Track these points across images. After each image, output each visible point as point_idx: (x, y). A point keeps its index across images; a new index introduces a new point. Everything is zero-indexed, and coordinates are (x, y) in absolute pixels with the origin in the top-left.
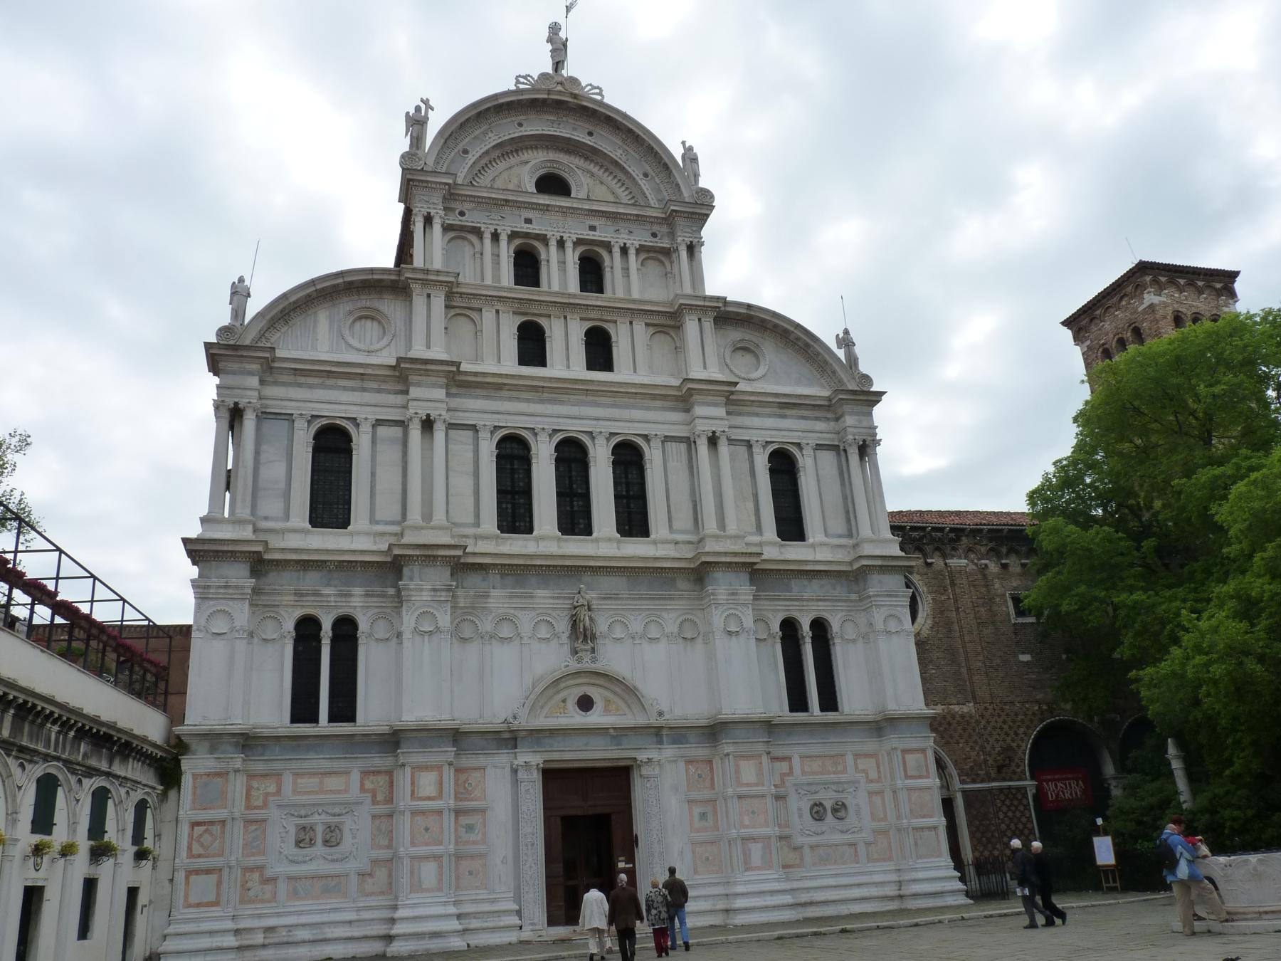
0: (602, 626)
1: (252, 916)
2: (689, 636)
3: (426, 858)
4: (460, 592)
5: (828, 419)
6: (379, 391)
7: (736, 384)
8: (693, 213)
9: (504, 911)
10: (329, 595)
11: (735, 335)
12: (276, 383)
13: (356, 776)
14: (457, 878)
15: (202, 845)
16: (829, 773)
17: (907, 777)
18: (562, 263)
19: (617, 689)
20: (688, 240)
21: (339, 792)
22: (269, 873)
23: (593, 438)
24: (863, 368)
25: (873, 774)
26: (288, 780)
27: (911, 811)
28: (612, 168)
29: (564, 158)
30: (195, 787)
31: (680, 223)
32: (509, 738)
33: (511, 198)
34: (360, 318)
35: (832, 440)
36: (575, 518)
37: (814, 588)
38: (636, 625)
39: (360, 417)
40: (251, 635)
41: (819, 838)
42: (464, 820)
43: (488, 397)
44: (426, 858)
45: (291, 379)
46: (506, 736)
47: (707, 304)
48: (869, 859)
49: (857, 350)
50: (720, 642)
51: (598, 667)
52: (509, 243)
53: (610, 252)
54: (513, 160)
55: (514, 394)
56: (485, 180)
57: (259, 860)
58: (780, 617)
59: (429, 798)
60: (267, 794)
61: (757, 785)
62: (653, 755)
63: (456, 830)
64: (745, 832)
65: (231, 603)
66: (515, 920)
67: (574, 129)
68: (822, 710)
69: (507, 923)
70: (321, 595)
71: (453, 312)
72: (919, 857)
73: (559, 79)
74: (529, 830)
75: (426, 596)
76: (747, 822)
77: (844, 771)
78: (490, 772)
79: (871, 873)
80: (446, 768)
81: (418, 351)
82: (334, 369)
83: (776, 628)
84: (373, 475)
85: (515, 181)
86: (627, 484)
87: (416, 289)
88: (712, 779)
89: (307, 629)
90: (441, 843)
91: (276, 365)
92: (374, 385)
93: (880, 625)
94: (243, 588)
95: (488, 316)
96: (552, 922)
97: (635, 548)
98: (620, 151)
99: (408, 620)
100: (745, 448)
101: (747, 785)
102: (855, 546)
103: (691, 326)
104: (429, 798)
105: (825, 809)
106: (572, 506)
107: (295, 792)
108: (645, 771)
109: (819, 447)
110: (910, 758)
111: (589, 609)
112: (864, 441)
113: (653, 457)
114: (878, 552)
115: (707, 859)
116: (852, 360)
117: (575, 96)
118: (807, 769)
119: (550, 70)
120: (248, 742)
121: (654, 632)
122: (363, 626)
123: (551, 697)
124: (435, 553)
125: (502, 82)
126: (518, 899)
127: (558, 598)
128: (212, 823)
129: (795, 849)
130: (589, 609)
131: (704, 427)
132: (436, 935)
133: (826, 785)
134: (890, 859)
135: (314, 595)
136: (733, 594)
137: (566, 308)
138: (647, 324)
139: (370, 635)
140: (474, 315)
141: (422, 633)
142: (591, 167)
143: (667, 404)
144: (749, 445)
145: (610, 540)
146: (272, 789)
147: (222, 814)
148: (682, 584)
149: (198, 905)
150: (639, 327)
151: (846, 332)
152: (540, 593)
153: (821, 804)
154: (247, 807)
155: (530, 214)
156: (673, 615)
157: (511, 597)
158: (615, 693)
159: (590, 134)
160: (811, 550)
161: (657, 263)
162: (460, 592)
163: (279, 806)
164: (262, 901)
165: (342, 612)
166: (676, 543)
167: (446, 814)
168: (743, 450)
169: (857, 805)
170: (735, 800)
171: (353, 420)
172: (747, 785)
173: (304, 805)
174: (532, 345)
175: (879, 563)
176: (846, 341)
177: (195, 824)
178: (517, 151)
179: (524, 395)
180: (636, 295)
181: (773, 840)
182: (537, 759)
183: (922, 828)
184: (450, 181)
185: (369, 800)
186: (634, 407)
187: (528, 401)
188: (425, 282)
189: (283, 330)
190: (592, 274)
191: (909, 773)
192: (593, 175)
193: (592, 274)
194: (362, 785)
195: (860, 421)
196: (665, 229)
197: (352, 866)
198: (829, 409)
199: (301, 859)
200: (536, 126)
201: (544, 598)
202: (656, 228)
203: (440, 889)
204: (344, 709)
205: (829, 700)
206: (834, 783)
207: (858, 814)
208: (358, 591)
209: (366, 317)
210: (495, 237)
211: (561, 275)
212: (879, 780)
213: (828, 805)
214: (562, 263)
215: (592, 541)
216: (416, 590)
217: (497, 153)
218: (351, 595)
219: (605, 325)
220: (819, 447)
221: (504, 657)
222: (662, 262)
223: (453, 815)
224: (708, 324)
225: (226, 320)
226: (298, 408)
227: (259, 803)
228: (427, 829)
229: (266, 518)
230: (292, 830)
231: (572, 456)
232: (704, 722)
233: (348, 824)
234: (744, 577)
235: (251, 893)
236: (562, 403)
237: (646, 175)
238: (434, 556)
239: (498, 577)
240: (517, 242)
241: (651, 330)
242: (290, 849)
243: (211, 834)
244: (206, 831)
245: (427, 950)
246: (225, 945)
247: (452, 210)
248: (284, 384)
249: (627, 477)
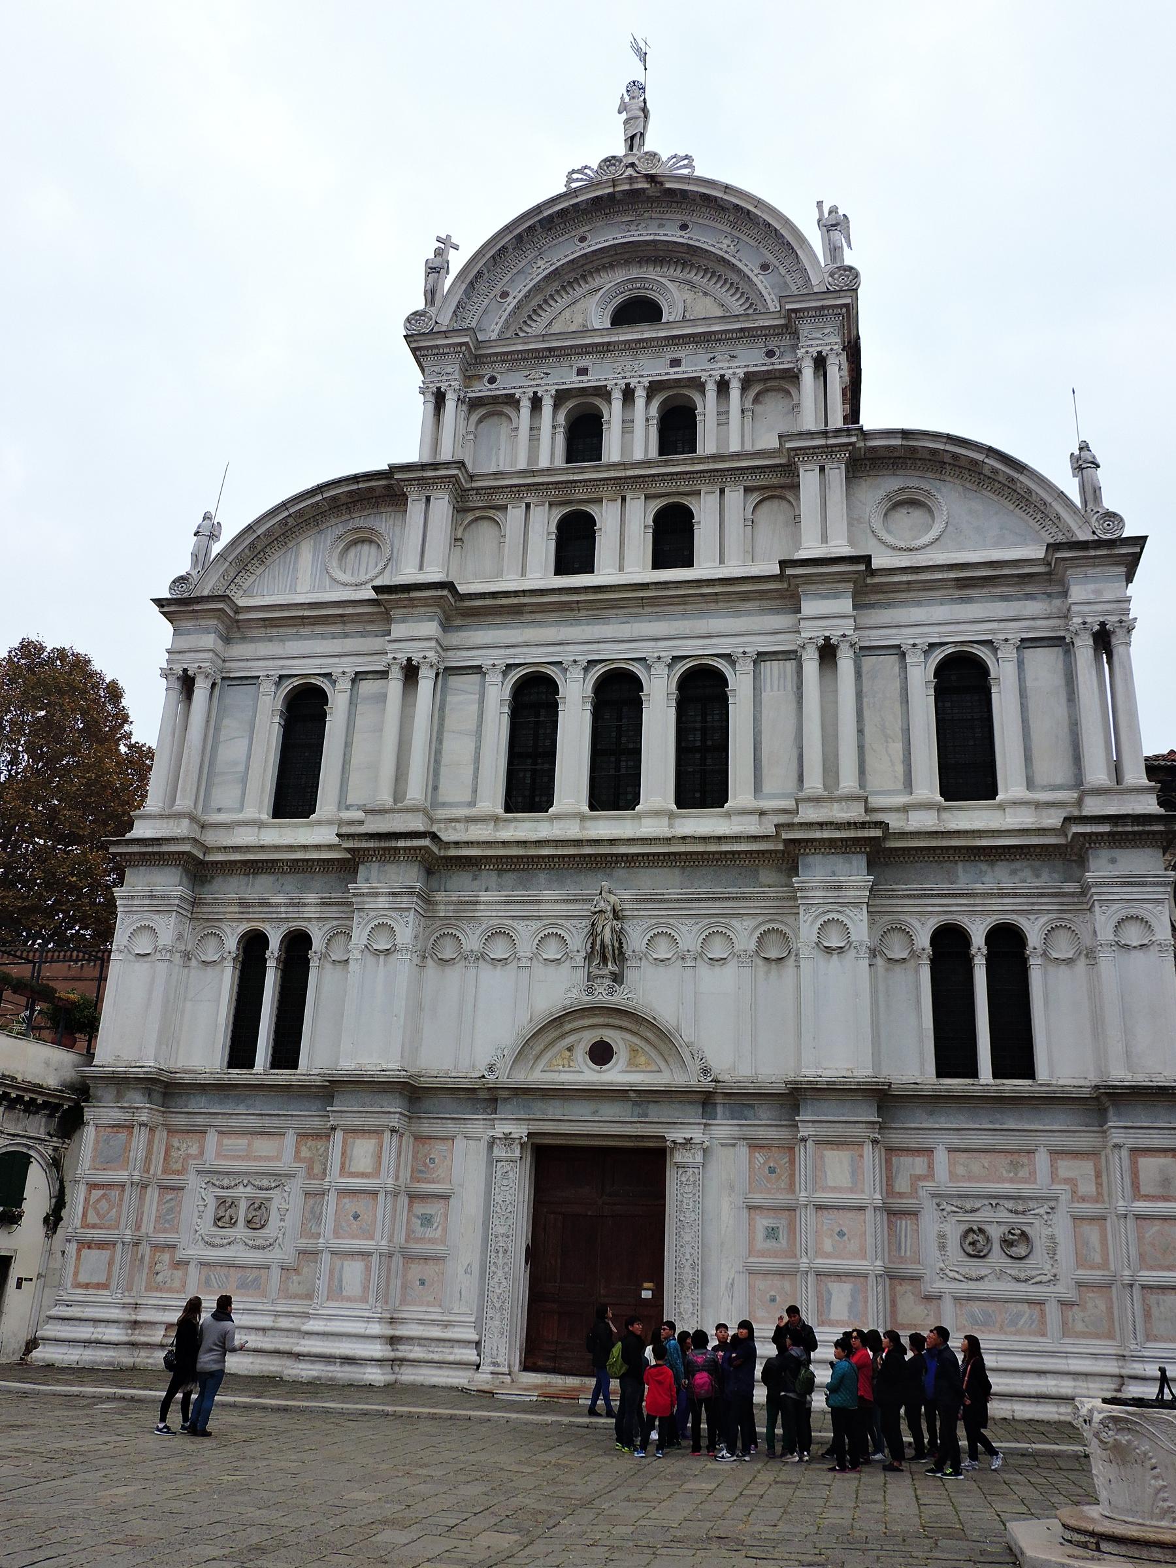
0: (636, 940)
1: (157, 1307)
2: (773, 954)
3: (351, 1254)
4: (439, 896)
5: (1049, 595)
6: (363, 635)
7: (867, 559)
8: (823, 308)
9: (458, 1341)
10: (279, 905)
11: (890, 483)
12: (244, 639)
13: (290, 1139)
14: (404, 1287)
15: (98, 1214)
16: (1001, 1180)
17: (1137, 1194)
18: (627, 423)
19: (649, 1035)
20: (814, 351)
21: (268, 1159)
22: (180, 1255)
23: (649, 667)
24: (1109, 502)
25: (1087, 1188)
26: (212, 1138)
27: (1141, 1256)
28: (720, 269)
29: (651, 273)
30: (97, 1142)
31: (804, 329)
32: (485, 1097)
34: (355, 543)
35: (1053, 629)
36: (614, 785)
37: (998, 877)
38: (689, 936)
39: (336, 672)
40: (187, 956)
41: (972, 1285)
42: (420, 1208)
43: (504, 625)
44: (351, 1254)
45: (261, 632)
46: (483, 1095)
47: (831, 441)
48: (1066, 1330)
49: (1103, 476)
50: (811, 964)
51: (618, 999)
52: (556, 407)
53: (703, 393)
54: (579, 291)
55: (538, 616)
56: (537, 328)
57: (171, 1237)
58: (933, 923)
59: (363, 1175)
60: (189, 1156)
61: (851, 1190)
62: (696, 1134)
63: (408, 1222)
64: (822, 1263)
65: (156, 917)
66: (470, 1355)
67: (661, 226)
68: (995, 1076)
69: (458, 1358)
70: (269, 905)
71: (470, 517)
72: (1149, 1337)
73: (631, 160)
74: (502, 1230)
75: (383, 902)
76: (828, 1245)
77: (1032, 1177)
78: (460, 1143)
79: (1066, 1355)
80: (387, 1134)
81: (408, 574)
82: (307, 613)
83: (923, 940)
84: (348, 745)
85: (579, 319)
86: (704, 731)
87: (412, 492)
88: (792, 1175)
89: (254, 944)
90: (373, 1239)
91: (241, 617)
92: (359, 628)
93: (1106, 933)
94: (169, 897)
95: (515, 513)
96: (527, 1367)
97: (702, 823)
98: (727, 241)
99: (360, 935)
100: (894, 659)
101: (834, 1189)
102: (1079, 802)
103: (809, 479)
104: (363, 1175)
105: (988, 1239)
106: (618, 769)
107: (218, 1155)
108: (679, 1157)
109: (1026, 643)
110: (1148, 1164)
111: (616, 915)
112: (1103, 624)
113: (740, 685)
114: (1111, 810)
115: (773, 1300)
116: (1091, 492)
117: (651, 178)
118: (960, 1170)
119: (620, 150)
120: (166, 1089)
121: (718, 949)
122: (318, 944)
123: (552, 1043)
124: (393, 844)
125: (545, 184)
126: (478, 1325)
127: (575, 901)
128: (110, 1186)
129: (928, 1298)
130: (616, 915)
131: (813, 632)
132: (348, 1360)
133: (994, 1200)
134: (1110, 1336)
135: (261, 904)
136: (839, 888)
137: (625, 483)
138: (747, 490)
139: (324, 956)
140: (497, 516)
141: (378, 953)
142: (691, 276)
143: (765, 604)
144: (899, 652)
145: (657, 814)
146: (194, 1150)
147: (121, 1176)
148: (767, 876)
149: (87, 1286)
150: (735, 496)
151: (1084, 447)
152: (547, 894)
153: (981, 1231)
154: (164, 1172)
155: (582, 362)
156: (750, 923)
157: (508, 902)
158: (647, 1040)
159: (684, 227)
160: (999, 813)
161: (781, 395)
162: (439, 896)
163: (199, 1172)
164: (170, 1290)
165: (294, 925)
166: (762, 813)
167: (381, 1196)
168: (892, 661)
169: (1052, 1238)
170: (811, 1210)
171: (328, 675)
172: (834, 1189)
173: (228, 1173)
174: (575, 544)
175: (1105, 828)
176: (1084, 463)
177: (93, 1186)
178: (584, 277)
179: (555, 616)
180: (735, 447)
181: (871, 1280)
182: (520, 1131)
183: (1162, 1288)
184: (466, 339)
185: (302, 1173)
186: (715, 613)
187: (557, 623)
188: (422, 482)
189: (258, 572)
190: (677, 427)
191: (1144, 1190)
192: (692, 286)
193: (677, 427)
194: (297, 1151)
195: (1098, 592)
196: (787, 341)
197: (275, 1256)
198: (1045, 578)
199: (218, 1241)
200: (607, 235)
201: (556, 902)
202: (772, 344)
203: (364, 1300)
204: (286, 1052)
205: (1016, 1055)
206: (1008, 1198)
207: (1052, 1253)
208: (311, 897)
209: (363, 541)
210: (536, 403)
211: (630, 437)
212: (1098, 1198)
213: (995, 1233)
214: (627, 423)
215: (633, 817)
216: (369, 894)
217: (556, 285)
218: (305, 904)
219: (685, 501)
220: (1026, 643)
221: (494, 984)
222: (788, 393)
223: (407, 1200)
224: (837, 475)
225: (183, 566)
226: (266, 668)
227: (178, 1166)
228: (356, 1217)
229: (219, 810)
230: (212, 1204)
231: (618, 695)
232: (781, 1089)
233: (277, 1200)
234: (860, 862)
235: (160, 1278)
236: (606, 620)
237: (765, 267)
238: (396, 848)
239: (494, 874)
240: (570, 404)
241: (755, 497)
242: (206, 1227)
243: (108, 1201)
244: (104, 1195)
245: (331, 1379)
246: (105, 1338)
247: (481, 377)
248: (253, 640)
249: (704, 721)
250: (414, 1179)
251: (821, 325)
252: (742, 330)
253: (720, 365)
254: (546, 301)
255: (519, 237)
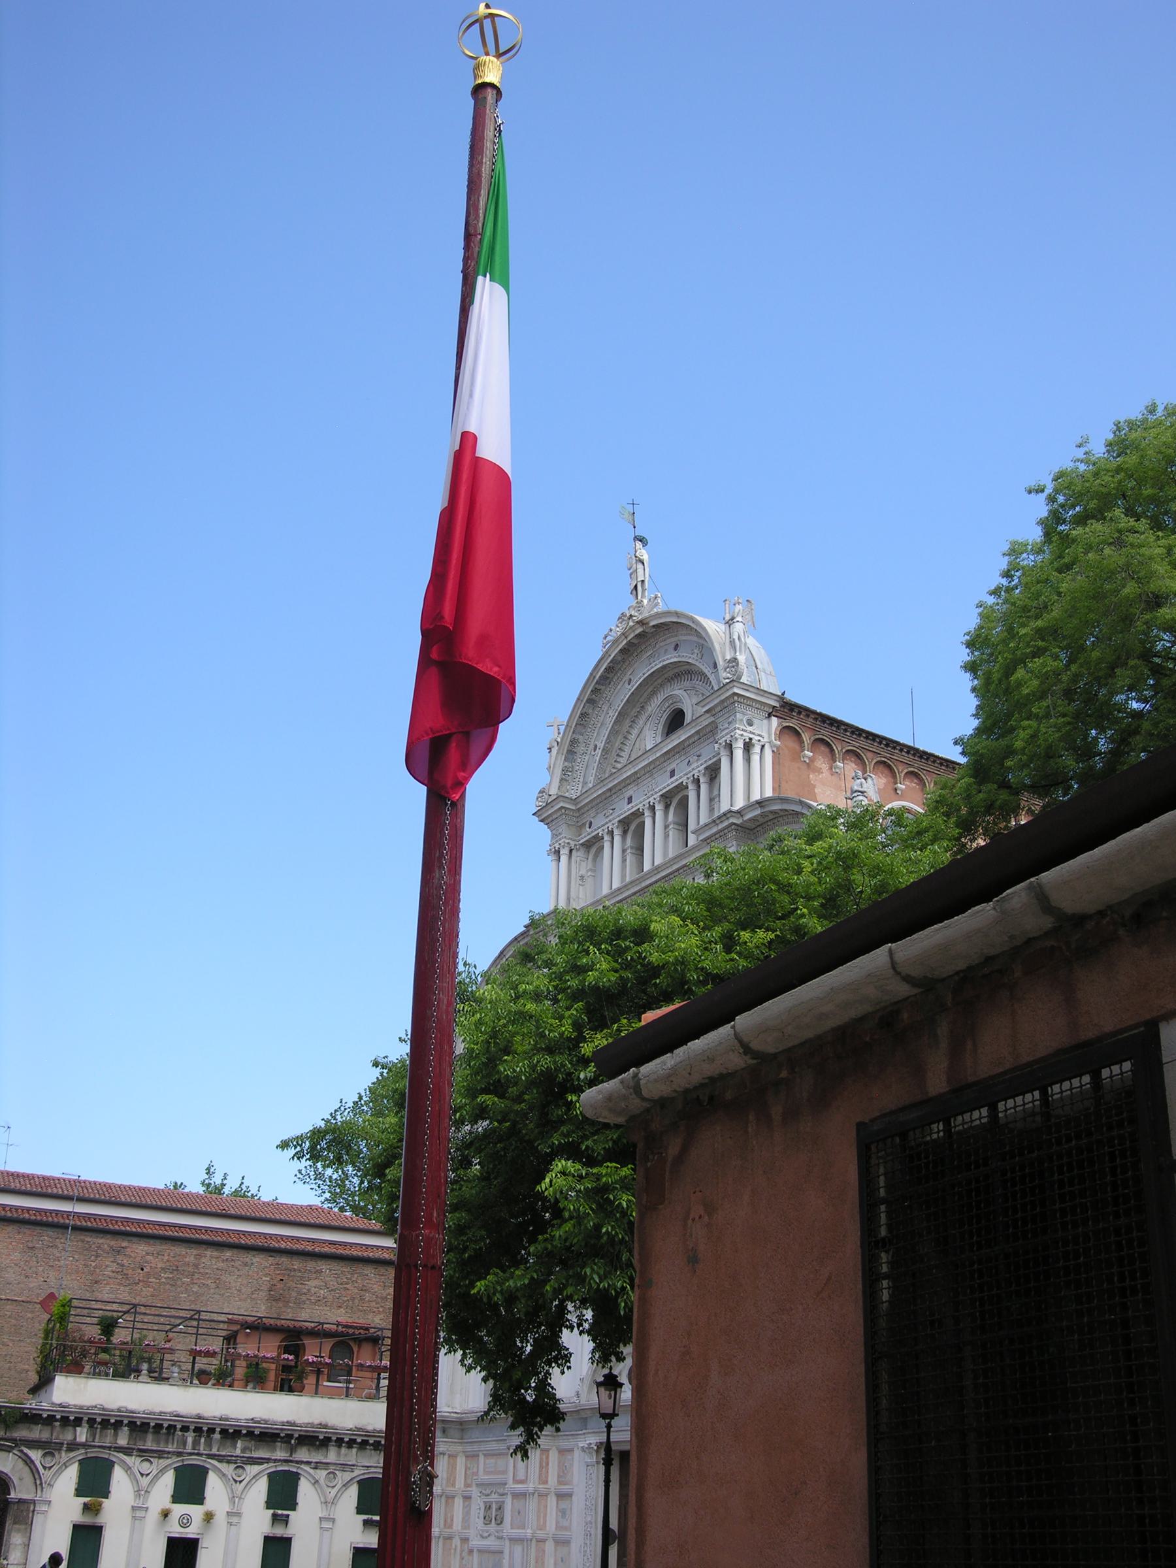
8: (722, 701)
26: (482, 1458)
33: (610, 785)
200: (641, 671)
217: (627, 723)
223: (554, 1498)
242: (480, 1523)
247: (584, 824)
250: (560, 1483)
251: (727, 715)
252: (697, 732)
253: (694, 766)
254: (626, 738)
255: (589, 701)
